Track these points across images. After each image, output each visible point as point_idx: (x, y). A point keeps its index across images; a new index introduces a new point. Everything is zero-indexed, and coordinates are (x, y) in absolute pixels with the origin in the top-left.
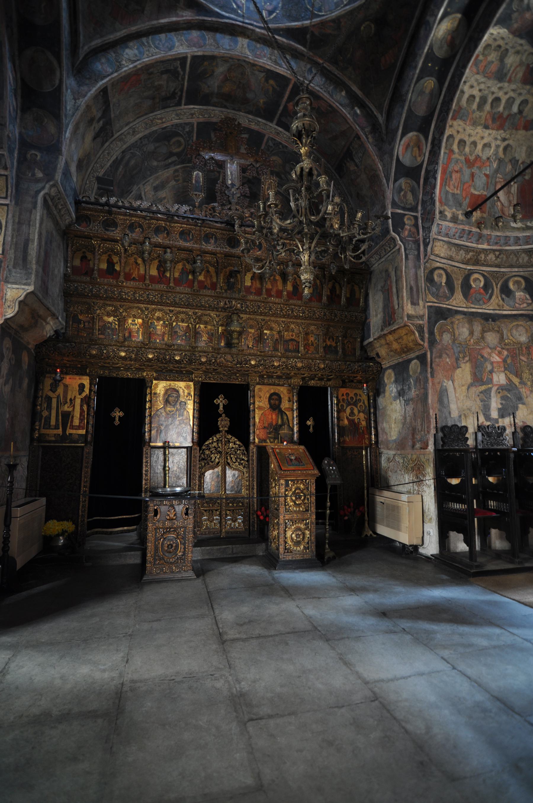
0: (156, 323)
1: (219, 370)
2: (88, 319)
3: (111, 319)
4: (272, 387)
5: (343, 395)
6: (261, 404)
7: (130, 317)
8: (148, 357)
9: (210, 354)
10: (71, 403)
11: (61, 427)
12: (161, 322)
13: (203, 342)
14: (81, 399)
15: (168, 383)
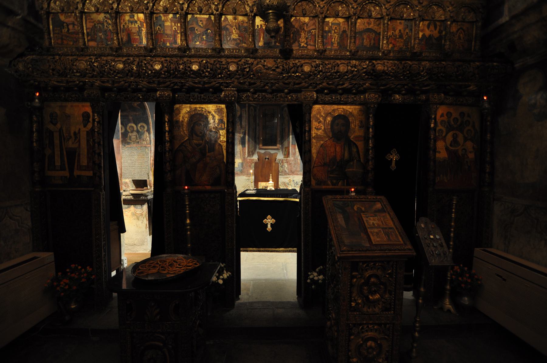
0: (163, 18)
1: (258, 84)
2: (72, 19)
3: (101, 17)
4: (336, 107)
5: (442, 115)
6: (320, 132)
7: (126, 13)
8: (156, 70)
9: (243, 60)
10: (76, 138)
11: (67, 169)
12: (171, 16)
13: (233, 42)
14: (87, 132)
15: (193, 106)
